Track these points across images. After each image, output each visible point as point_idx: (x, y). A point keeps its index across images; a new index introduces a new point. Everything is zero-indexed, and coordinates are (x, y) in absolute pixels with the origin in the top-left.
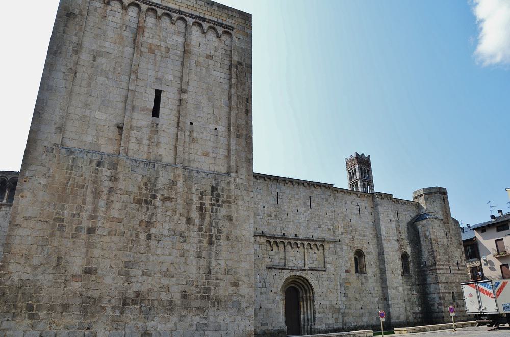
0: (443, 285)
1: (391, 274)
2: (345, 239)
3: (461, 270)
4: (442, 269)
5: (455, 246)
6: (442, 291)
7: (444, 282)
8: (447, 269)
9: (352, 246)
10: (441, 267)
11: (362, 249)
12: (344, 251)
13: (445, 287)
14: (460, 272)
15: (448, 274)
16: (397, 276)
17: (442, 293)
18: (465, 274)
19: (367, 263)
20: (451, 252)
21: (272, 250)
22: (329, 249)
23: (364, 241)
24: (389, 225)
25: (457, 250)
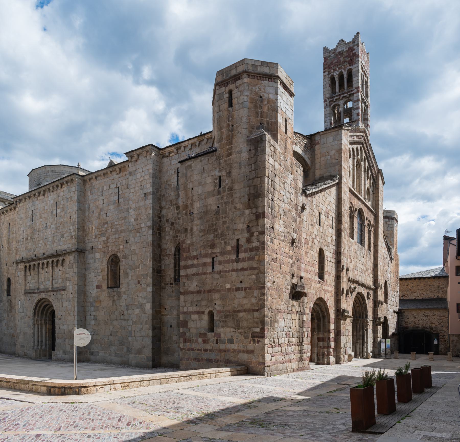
0: (189, 297)
1: (136, 285)
2: (99, 243)
3: (244, 260)
4: (193, 266)
5: (239, 206)
6: (185, 310)
7: (192, 293)
8: (204, 264)
9: (106, 250)
10: (190, 262)
11: (117, 252)
12: (97, 261)
13: (192, 303)
14: (240, 265)
15: (204, 274)
16: (145, 286)
17: (184, 313)
18: (254, 268)
19: (122, 272)
20: (225, 223)
21: (30, 275)
22: (70, 263)
23: (120, 239)
24: (142, 204)
25: (243, 214)
